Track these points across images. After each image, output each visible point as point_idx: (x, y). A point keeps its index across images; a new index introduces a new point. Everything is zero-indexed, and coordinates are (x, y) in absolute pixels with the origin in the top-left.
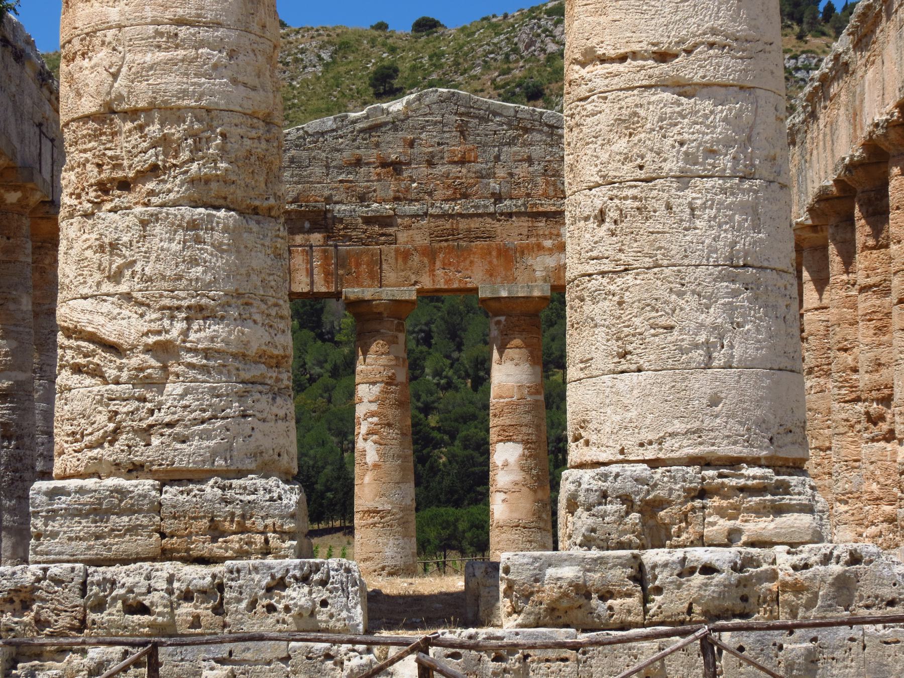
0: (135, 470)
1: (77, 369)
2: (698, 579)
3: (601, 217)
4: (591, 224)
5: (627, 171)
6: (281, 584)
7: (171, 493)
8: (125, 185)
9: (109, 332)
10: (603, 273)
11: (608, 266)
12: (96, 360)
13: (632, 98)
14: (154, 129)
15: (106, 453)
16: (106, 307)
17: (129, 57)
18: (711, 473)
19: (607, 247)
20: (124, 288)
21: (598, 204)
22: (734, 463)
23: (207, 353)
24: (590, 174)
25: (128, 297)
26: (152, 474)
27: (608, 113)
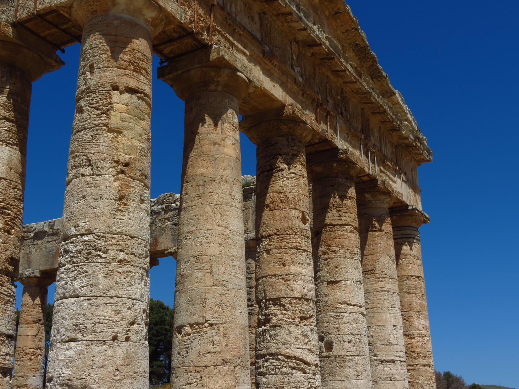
1: (294, 368)
3: (350, 342)
4: (347, 343)
5: (356, 332)
8: (305, 318)
10: (352, 356)
11: (354, 354)
12: (302, 366)
16: (306, 352)
17: (307, 284)
19: (353, 349)
20: (309, 347)
21: (350, 339)
24: (347, 331)
25: (309, 350)
27: (351, 318)
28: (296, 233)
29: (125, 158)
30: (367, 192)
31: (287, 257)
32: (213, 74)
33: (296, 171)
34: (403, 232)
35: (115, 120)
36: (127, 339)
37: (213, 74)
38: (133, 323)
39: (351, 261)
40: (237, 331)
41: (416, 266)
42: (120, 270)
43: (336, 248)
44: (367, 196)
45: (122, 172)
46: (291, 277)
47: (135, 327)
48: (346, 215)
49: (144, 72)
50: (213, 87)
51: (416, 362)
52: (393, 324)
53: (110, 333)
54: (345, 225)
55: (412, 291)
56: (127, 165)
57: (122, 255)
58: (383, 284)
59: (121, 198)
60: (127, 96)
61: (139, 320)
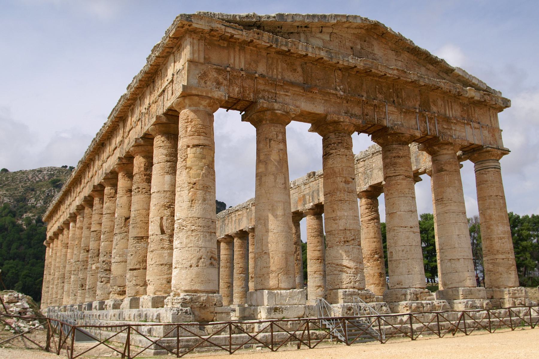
0: (354, 288)
2: (429, 305)
3: (403, 251)
6: (382, 306)
7: (360, 292)
8: (347, 241)
9: (348, 265)
13: (408, 234)
14: (353, 233)
15: (349, 285)
26: (357, 289)
28: (341, 191)
29: (193, 180)
30: (435, 146)
31: (335, 206)
32: (262, 115)
33: (340, 153)
34: (484, 165)
35: (189, 163)
36: (197, 266)
37: (262, 115)
38: (201, 258)
39: (403, 199)
40: (280, 255)
41: (495, 188)
42: (193, 234)
43: (392, 192)
44: (435, 148)
45: (193, 187)
46: (338, 218)
47: (203, 260)
48: (399, 169)
49: (203, 134)
50: (264, 122)
51: (497, 257)
52: (457, 234)
53: (189, 264)
55: (491, 207)
56: (195, 184)
57: (193, 228)
58: (448, 208)
59: (192, 201)
60: (195, 148)
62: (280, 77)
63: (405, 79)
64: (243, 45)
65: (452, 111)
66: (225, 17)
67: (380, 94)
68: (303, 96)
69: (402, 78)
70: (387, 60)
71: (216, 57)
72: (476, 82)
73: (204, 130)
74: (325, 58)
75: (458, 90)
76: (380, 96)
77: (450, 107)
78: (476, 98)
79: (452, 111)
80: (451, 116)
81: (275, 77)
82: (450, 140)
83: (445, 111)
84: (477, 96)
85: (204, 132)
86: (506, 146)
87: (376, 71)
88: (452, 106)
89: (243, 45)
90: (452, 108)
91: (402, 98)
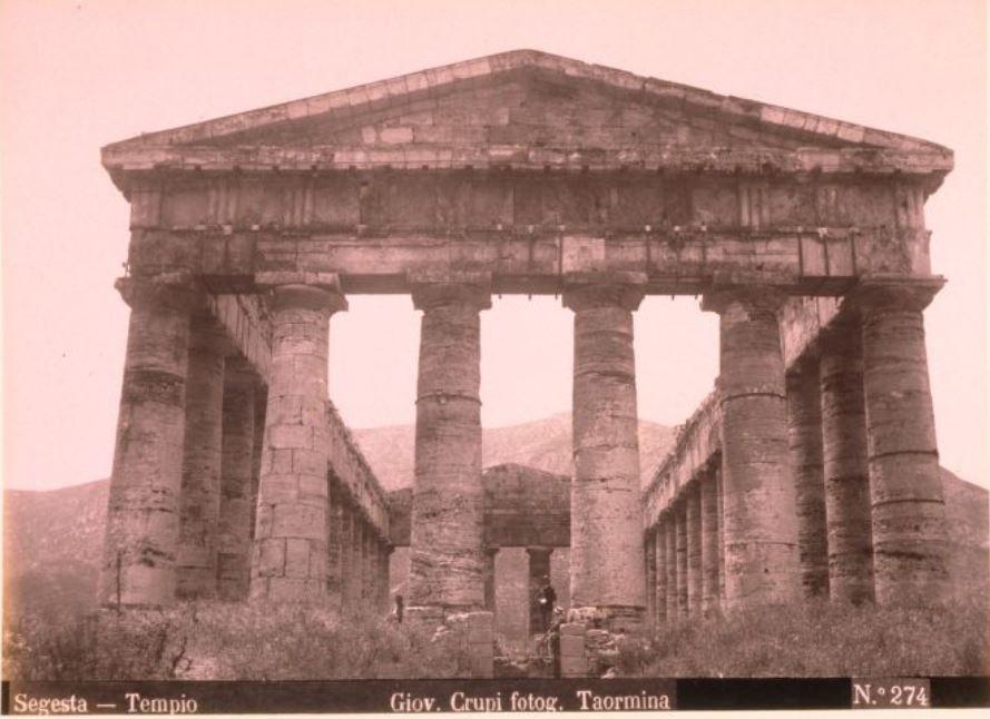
18: (615, 610)
22: (622, 607)
23: (459, 568)
49: (147, 347)
54: (586, 373)
61: (129, 549)
62: (306, 221)
63: (601, 167)
64: (234, 179)
65: (760, 212)
66: (184, 138)
67: (552, 209)
68: (357, 247)
69: (591, 168)
70: (581, 133)
71: (185, 213)
72: (832, 130)
73: (150, 341)
74: (395, 166)
75: (764, 161)
76: (551, 215)
77: (755, 202)
78: (825, 170)
79: (760, 212)
80: (756, 222)
81: (297, 223)
82: (735, 280)
83: (739, 213)
84: (831, 161)
85: (149, 344)
86: (936, 269)
87: (524, 166)
88: (760, 200)
89: (234, 179)
90: (759, 206)
91: (609, 207)
